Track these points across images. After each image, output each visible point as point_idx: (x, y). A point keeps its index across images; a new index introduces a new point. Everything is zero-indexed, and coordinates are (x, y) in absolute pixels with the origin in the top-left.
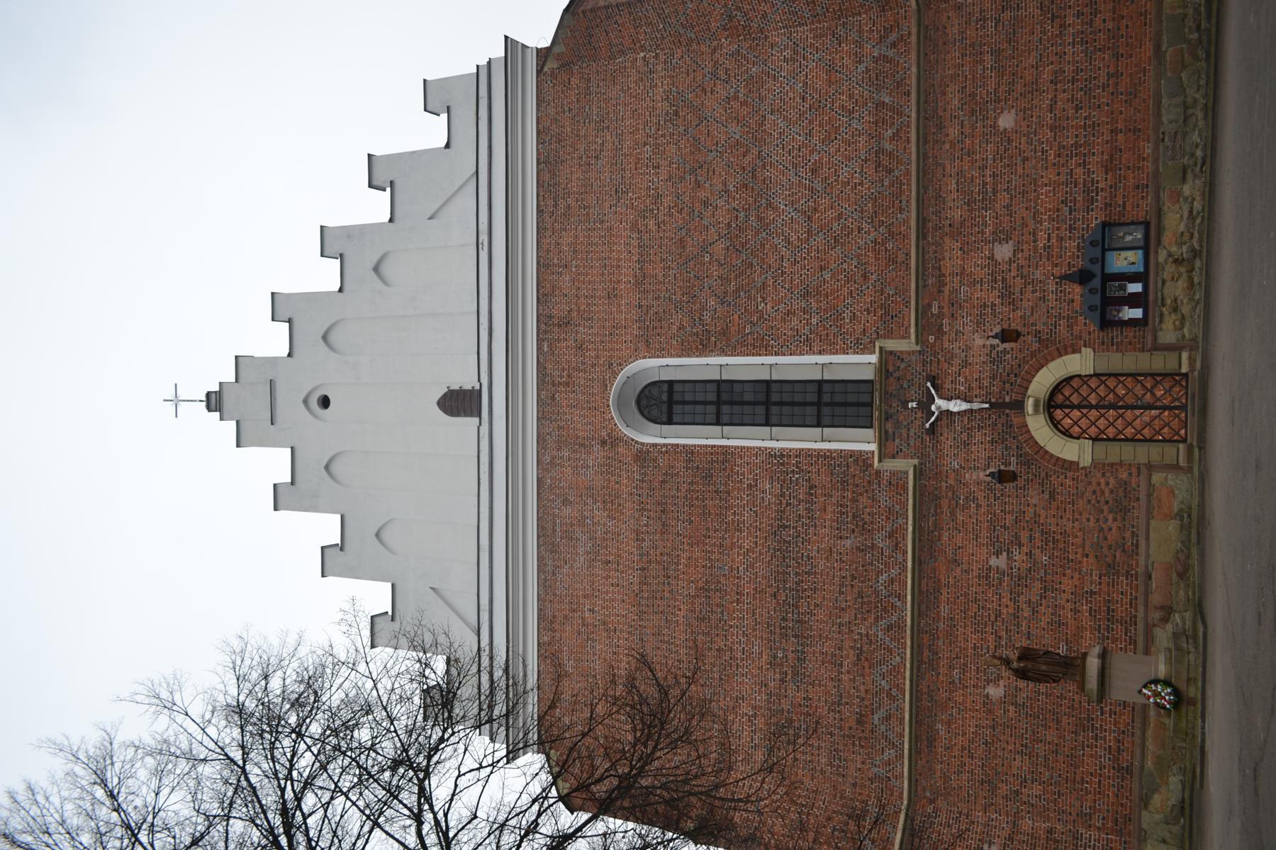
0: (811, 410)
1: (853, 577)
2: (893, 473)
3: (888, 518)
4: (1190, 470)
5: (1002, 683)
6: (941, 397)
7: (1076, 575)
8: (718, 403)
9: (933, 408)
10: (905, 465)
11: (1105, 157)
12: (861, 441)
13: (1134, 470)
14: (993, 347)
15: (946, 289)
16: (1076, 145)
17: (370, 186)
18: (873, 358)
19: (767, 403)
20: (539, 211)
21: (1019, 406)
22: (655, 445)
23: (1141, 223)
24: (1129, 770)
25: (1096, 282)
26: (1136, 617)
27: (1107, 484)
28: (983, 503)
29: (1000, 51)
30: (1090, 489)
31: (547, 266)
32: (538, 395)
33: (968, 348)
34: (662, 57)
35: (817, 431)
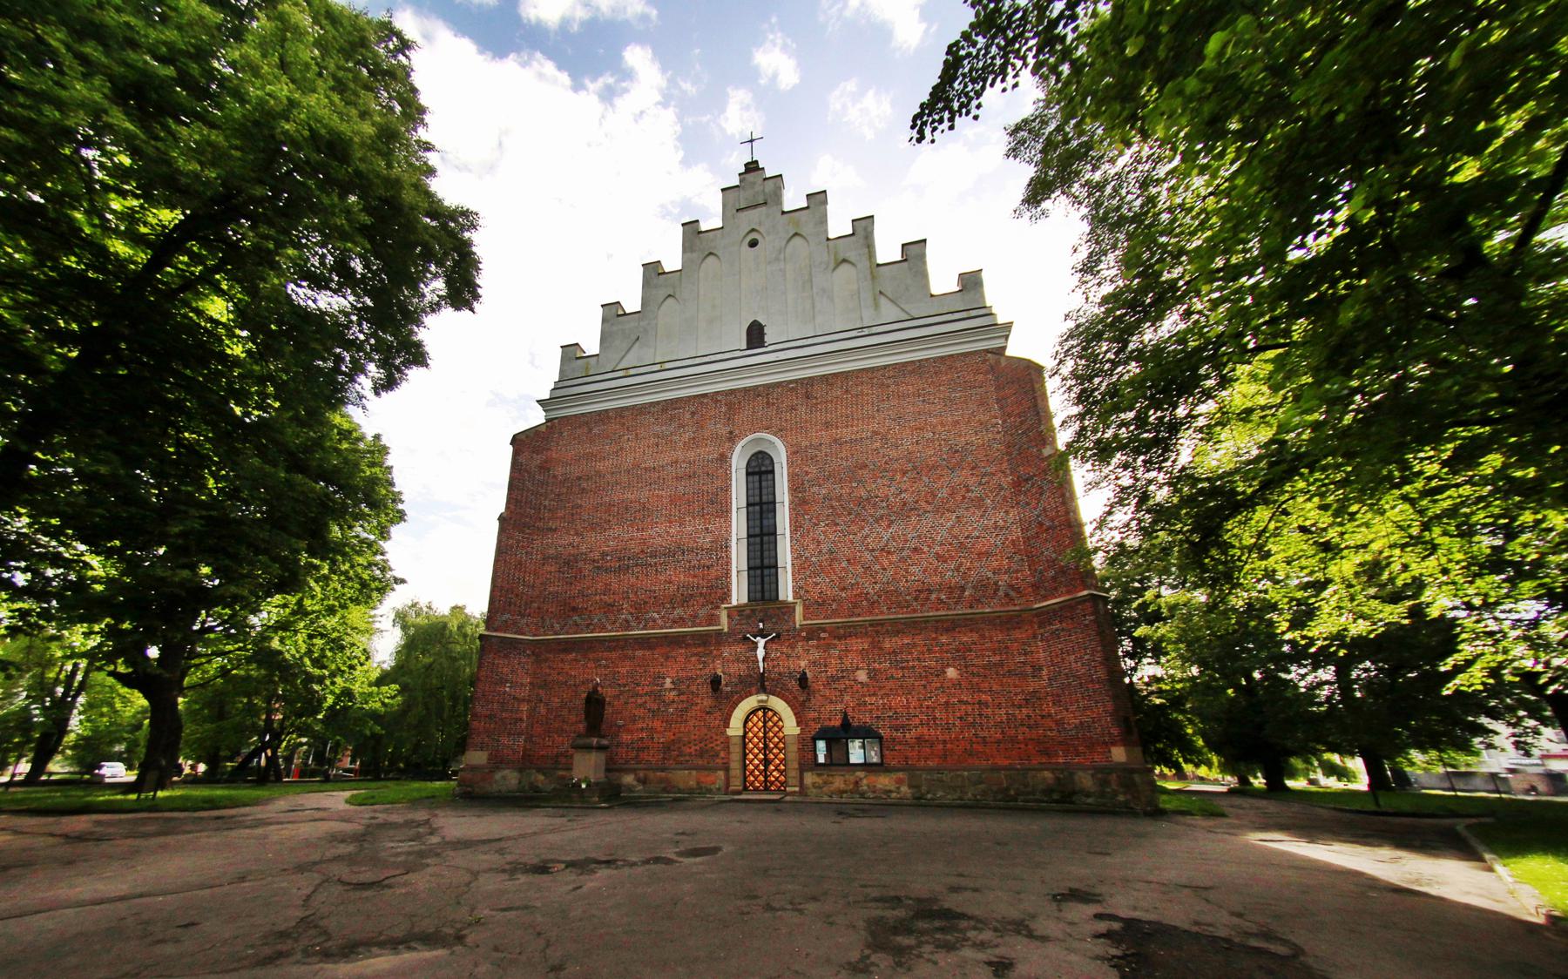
0: (758, 562)
2: (718, 617)
8: (761, 504)
10: (724, 624)
12: (739, 593)
18: (790, 599)
19: (762, 535)
21: (763, 689)
33: (798, 658)
35: (746, 568)
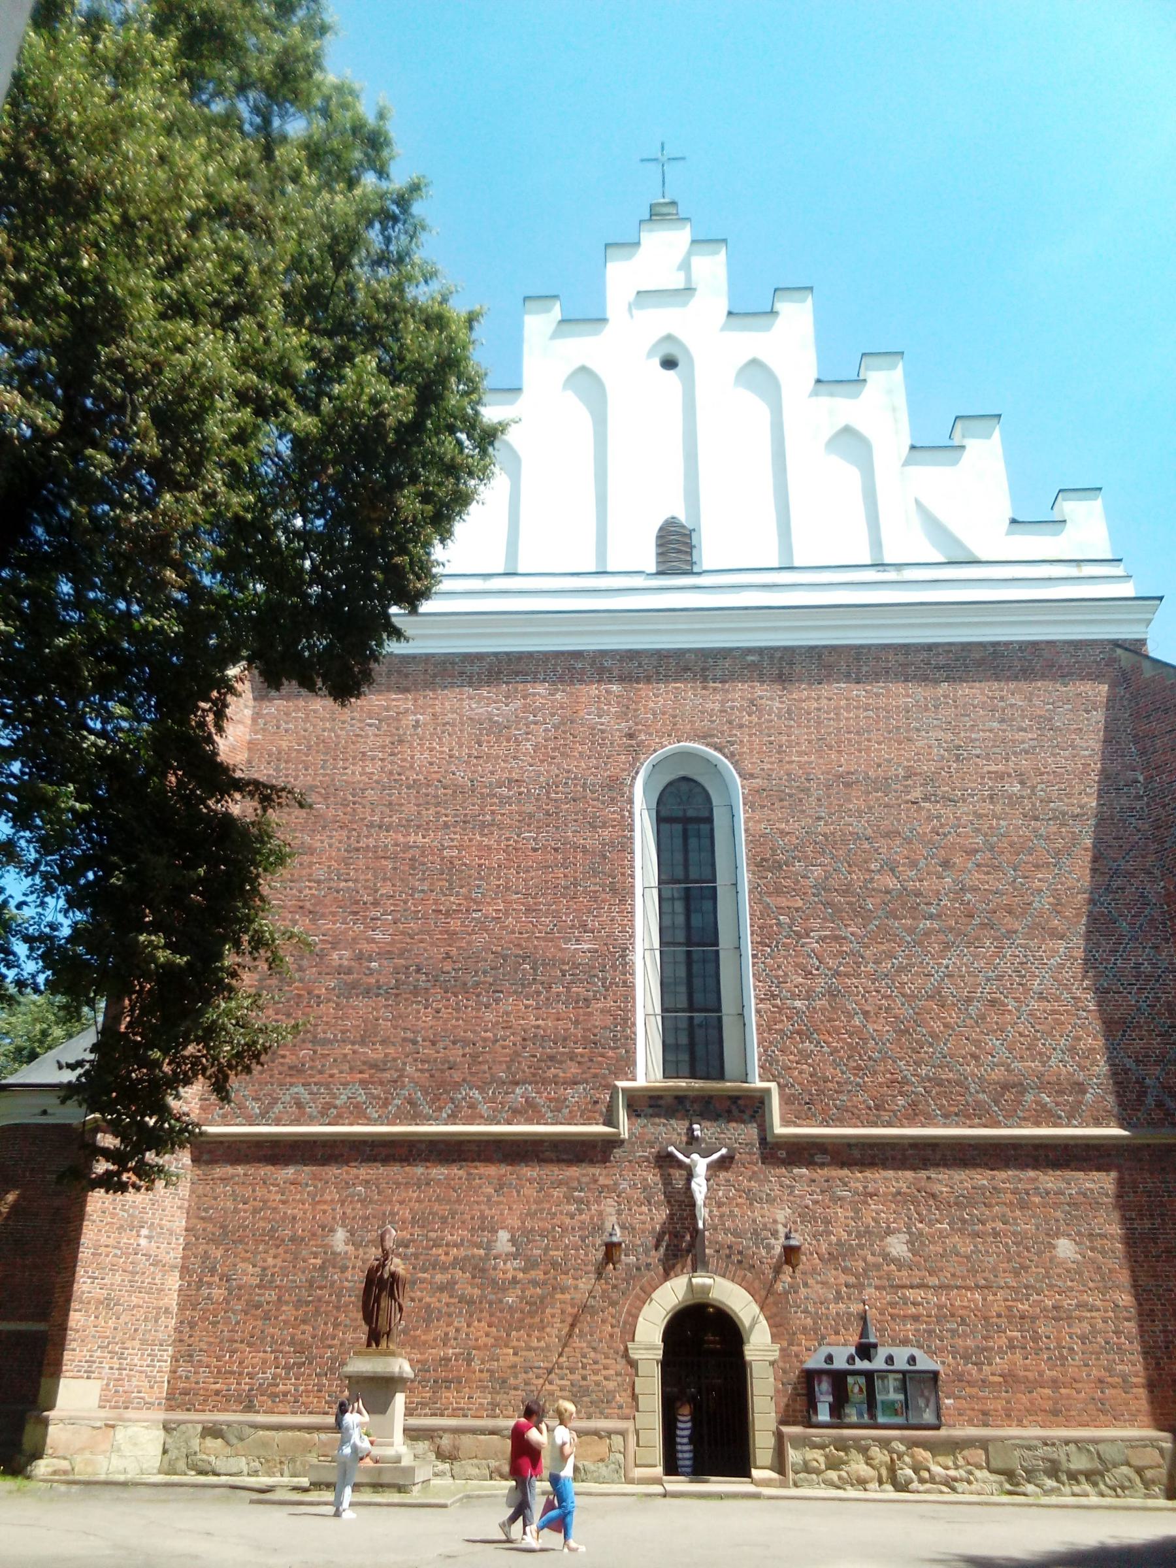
1: (474, 1057)
3: (551, 1100)
4: (630, 1481)
5: (350, 1248)
6: (710, 1166)
7: (491, 1341)
9: (695, 1156)
11: (1022, 1373)
13: (626, 1411)
14: (775, 1234)
15: (845, 1172)
16: (1036, 1338)
17: (957, 418)
20: (930, 647)
22: (631, 801)
23: (938, 1417)
24: (249, 1408)
25: (861, 1365)
26: (442, 1415)
27: (606, 1378)
28: (575, 1223)
29: (1155, 1241)
30: (601, 1357)
31: (858, 660)
32: (689, 650)
33: (771, 1200)
34: (1138, 805)
